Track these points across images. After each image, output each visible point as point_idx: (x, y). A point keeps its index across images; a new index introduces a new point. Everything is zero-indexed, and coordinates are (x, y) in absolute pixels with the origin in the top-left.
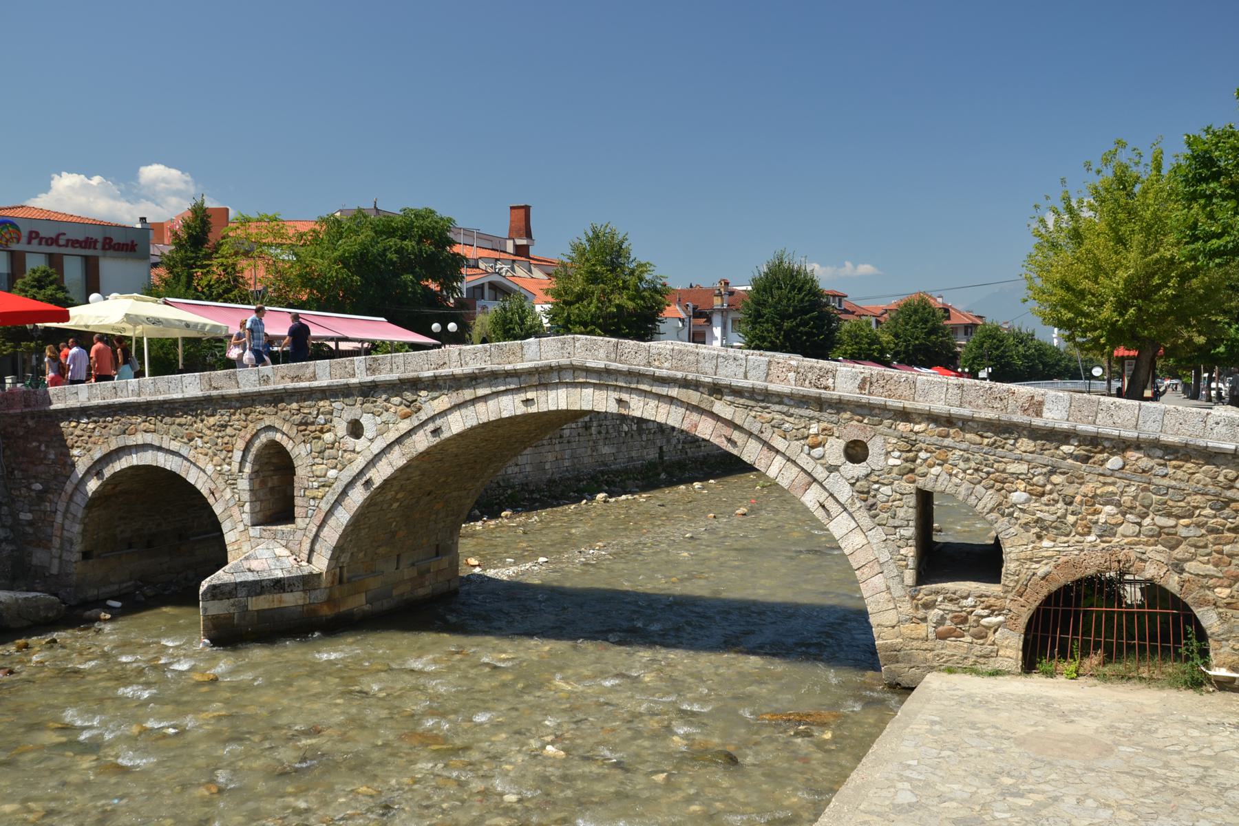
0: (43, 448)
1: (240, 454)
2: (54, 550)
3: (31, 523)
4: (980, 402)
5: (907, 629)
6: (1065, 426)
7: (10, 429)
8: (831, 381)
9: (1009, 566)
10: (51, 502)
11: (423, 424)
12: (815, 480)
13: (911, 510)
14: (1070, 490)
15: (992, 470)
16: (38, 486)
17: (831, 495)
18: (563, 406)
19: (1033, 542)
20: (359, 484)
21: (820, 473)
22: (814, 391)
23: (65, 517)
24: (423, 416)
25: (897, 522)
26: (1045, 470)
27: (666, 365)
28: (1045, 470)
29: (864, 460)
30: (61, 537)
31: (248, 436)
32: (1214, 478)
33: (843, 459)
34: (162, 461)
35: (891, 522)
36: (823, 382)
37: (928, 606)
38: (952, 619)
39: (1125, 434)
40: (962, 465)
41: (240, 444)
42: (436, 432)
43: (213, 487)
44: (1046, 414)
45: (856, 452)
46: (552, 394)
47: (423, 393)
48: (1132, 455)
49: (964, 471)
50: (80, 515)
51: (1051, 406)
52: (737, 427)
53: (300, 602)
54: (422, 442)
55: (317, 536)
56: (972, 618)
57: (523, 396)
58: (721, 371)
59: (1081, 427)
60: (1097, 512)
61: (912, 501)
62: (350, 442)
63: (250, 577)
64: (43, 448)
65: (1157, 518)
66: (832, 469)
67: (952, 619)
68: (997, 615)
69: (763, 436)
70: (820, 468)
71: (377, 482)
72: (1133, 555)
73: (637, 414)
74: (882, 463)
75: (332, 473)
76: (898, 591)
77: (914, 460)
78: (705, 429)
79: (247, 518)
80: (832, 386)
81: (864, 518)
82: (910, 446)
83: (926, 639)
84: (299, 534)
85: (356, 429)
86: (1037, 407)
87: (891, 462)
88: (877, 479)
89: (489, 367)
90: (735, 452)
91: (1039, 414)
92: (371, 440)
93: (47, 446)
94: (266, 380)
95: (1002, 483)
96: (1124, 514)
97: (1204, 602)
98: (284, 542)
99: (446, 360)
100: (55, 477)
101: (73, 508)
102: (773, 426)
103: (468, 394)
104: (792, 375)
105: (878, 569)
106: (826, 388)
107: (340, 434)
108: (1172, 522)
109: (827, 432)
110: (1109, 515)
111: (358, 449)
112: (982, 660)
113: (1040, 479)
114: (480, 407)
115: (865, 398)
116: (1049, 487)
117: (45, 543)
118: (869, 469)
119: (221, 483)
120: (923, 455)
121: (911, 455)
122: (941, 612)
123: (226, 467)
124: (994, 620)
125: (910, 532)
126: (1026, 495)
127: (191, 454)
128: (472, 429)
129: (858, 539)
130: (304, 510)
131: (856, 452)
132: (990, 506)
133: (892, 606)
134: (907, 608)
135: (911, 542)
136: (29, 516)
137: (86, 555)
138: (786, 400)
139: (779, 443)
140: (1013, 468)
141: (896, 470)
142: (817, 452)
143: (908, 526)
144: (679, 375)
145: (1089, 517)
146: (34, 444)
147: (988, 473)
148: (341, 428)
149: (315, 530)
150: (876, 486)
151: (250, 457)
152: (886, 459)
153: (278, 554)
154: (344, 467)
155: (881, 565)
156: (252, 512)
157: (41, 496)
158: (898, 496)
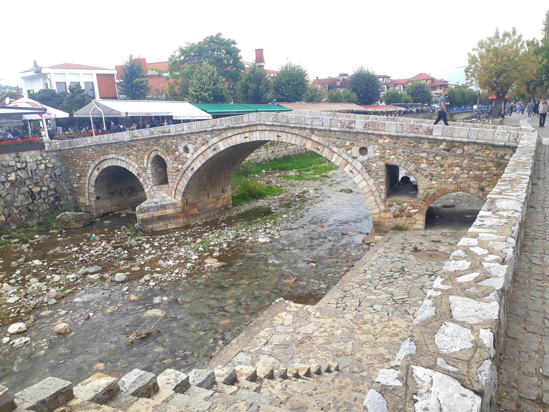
0: (78, 161)
1: (147, 160)
2: (87, 197)
3: (77, 188)
4: (409, 130)
5: (383, 215)
6: (441, 138)
7: (66, 155)
8: (354, 125)
9: (421, 191)
11: (209, 147)
12: (348, 162)
13: (383, 172)
14: (442, 163)
15: (414, 156)
16: (78, 175)
17: (354, 167)
18: (258, 139)
19: (429, 182)
22: (347, 130)
24: (209, 144)
25: (378, 177)
26: (433, 155)
27: (294, 122)
28: (433, 155)
29: (366, 154)
30: (89, 193)
31: (149, 154)
32: (496, 155)
33: (359, 154)
34: (119, 164)
35: (376, 177)
37: (390, 206)
38: (399, 211)
40: (402, 155)
41: (146, 157)
42: (214, 150)
43: (138, 173)
44: (434, 133)
46: (254, 135)
47: (209, 136)
48: (466, 148)
49: (403, 157)
50: (94, 184)
51: (436, 131)
52: (320, 144)
53: (173, 212)
54: (210, 154)
55: (176, 189)
56: (406, 210)
57: (243, 136)
58: (314, 124)
59: (447, 138)
60: (453, 170)
61: (384, 168)
62: (185, 155)
63: (154, 205)
64: (78, 161)
65: (475, 171)
66: (354, 158)
67: (399, 211)
68: (415, 209)
70: (350, 158)
71: (196, 169)
72: (466, 185)
73: (285, 141)
74: (373, 155)
75: (180, 166)
76: (379, 201)
77: (384, 153)
80: (354, 127)
81: (367, 176)
83: (390, 218)
84: (170, 189)
85: (186, 150)
87: (376, 154)
88: (371, 161)
89: (231, 126)
91: (431, 134)
93: (79, 160)
95: (417, 161)
96: (462, 170)
98: (165, 192)
99: (216, 123)
100: (83, 171)
101: (91, 182)
102: (333, 143)
103: (224, 135)
104: (339, 124)
105: (371, 194)
106: (352, 128)
107: (181, 152)
108: (480, 173)
109: (352, 144)
110: (457, 171)
111: (188, 157)
112: (410, 225)
113: (431, 159)
115: (366, 131)
116: (435, 162)
117: (83, 195)
118: (368, 158)
119: (141, 171)
120: (388, 151)
121: (383, 151)
122: (395, 208)
123: (142, 166)
124: (414, 211)
125: (383, 180)
126: (426, 165)
128: (227, 149)
129: (364, 183)
130: (171, 180)
131: (363, 151)
132: (413, 169)
133: (377, 207)
134: (382, 207)
135: (384, 184)
136: (76, 185)
137: (98, 198)
138: (337, 133)
141: (378, 157)
143: (383, 177)
144: (299, 126)
145: (450, 172)
147: (412, 157)
148: (181, 149)
149: (176, 187)
150: (371, 164)
151: (150, 161)
152: (374, 154)
153: (163, 196)
154: (184, 164)
155: (373, 192)
156: (153, 181)
158: (379, 167)
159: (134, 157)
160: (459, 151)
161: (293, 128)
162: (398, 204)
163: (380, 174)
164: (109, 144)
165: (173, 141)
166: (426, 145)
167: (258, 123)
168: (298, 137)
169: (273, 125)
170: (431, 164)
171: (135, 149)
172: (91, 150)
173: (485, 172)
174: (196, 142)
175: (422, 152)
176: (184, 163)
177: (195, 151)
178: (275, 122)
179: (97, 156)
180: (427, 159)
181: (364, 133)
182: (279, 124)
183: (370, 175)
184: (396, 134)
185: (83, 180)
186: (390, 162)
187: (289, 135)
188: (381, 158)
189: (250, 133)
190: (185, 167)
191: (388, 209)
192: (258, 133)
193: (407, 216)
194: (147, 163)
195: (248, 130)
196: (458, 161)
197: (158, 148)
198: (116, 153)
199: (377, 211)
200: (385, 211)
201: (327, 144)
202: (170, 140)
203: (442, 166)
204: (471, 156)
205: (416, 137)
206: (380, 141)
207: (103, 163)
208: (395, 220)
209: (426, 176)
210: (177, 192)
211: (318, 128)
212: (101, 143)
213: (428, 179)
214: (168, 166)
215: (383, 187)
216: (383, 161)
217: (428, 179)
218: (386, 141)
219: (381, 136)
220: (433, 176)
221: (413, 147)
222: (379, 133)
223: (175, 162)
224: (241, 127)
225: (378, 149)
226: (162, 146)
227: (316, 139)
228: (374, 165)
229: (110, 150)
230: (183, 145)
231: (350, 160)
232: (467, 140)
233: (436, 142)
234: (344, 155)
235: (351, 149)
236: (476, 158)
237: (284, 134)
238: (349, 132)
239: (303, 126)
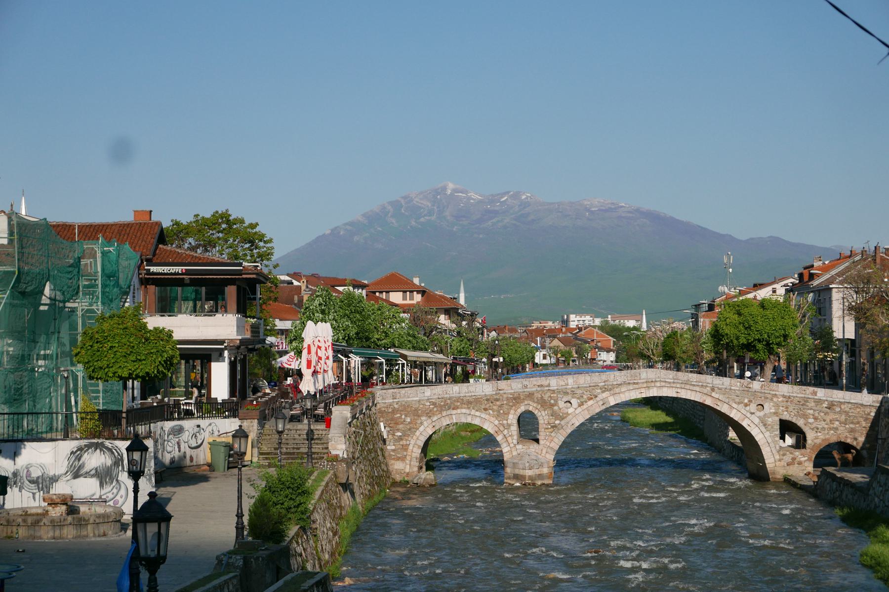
0: (403, 417)
2: (407, 462)
3: (393, 450)
4: (798, 391)
5: (778, 463)
6: (824, 399)
10: (406, 440)
16: (399, 434)
18: (655, 395)
20: (569, 425)
23: (413, 447)
27: (695, 380)
32: (864, 412)
36: (749, 386)
37: (784, 455)
39: (841, 400)
44: (818, 395)
46: (651, 391)
48: (843, 407)
59: (829, 399)
60: (833, 424)
61: (778, 423)
64: (403, 417)
66: (752, 413)
69: (729, 403)
70: (748, 413)
73: (684, 397)
74: (768, 411)
75: (557, 422)
78: (708, 402)
79: (515, 442)
82: (777, 405)
86: (815, 393)
87: (771, 411)
90: (719, 409)
91: (816, 395)
92: (576, 409)
94: (526, 387)
95: (805, 416)
100: (410, 429)
103: (617, 390)
104: (738, 384)
109: (750, 401)
111: (569, 412)
113: (817, 415)
115: (763, 391)
119: (502, 428)
120: (781, 408)
123: (505, 422)
129: (761, 436)
134: (777, 457)
136: (393, 447)
142: (748, 408)
144: (700, 384)
146: (398, 415)
157: (400, 438)
159: (493, 412)
160: (838, 409)
162: (791, 453)
163: (775, 427)
165: (552, 395)
166: (813, 404)
167: (659, 379)
168: (698, 393)
169: (674, 383)
170: (816, 419)
171: (498, 403)
172: (429, 404)
173: (857, 425)
174: (582, 397)
175: (809, 409)
176: (562, 419)
177: (580, 406)
178: (676, 379)
179: (436, 411)
180: (813, 415)
181: (761, 393)
182: (681, 382)
183: (766, 428)
184: (788, 394)
186: (784, 418)
187: (689, 391)
188: (776, 413)
189: (646, 389)
191: (781, 457)
192: (655, 389)
193: (798, 464)
194: (513, 419)
195: (645, 385)
196: (837, 416)
197: (531, 403)
198: (469, 408)
199: (772, 460)
200: (780, 460)
201: (727, 401)
202: (548, 394)
203: (824, 421)
204: (847, 413)
205: (805, 397)
206: (775, 399)
208: (788, 467)
209: (813, 429)
211: (720, 386)
212: (446, 396)
213: (814, 432)
214: (541, 422)
216: (777, 416)
217: (814, 432)
218: (779, 400)
220: (818, 429)
221: (802, 405)
222: (774, 393)
223: (551, 417)
224: (637, 383)
225: (773, 406)
226: (536, 401)
227: (717, 396)
228: (770, 420)
229: (459, 404)
230: (565, 399)
231: (749, 415)
232: (844, 400)
233: (819, 402)
234: (743, 411)
235: (749, 405)
236: (850, 414)
237: (683, 390)
239: (704, 384)
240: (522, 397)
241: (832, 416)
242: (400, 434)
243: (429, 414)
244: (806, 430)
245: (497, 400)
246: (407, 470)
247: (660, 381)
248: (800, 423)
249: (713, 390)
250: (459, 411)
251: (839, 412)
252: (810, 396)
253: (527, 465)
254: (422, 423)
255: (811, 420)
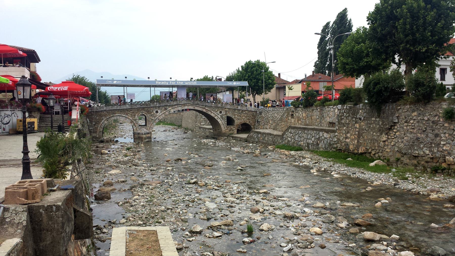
20: (157, 119)
21: (217, 115)
23: (100, 128)
41: (137, 115)
45: (221, 112)
46: (185, 107)
47: (168, 107)
48: (246, 112)
62: (156, 114)
64: (95, 117)
66: (218, 114)
75: (153, 118)
76: (225, 127)
78: (204, 111)
82: (226, 111)
84: (147, 127)
85: (157, 112)
86: (238, 107)
95: (235, 115)
97: (252, 125)
103: (174, 107)
114: (176, 109)
125: (226, 120)
127: (127, 117)
131: (221, 112)
134: (226, 129)
139: (213, 112)
140: (236, 113)
142: (217, 112)
148: (155, 112)
157: (94, 125)
160: (244, 112)
161: (200, 105)
164: (117, 109)
166: (237, 111)
171: (131, 112)
177: (161, 112)
185: (97, 125)
188: (226, 114)
190: (155, 118)
192: (187, 106)
195: (183, 105)
200: (227, 130)
207: (111, 118)
210: (150, 128)
215: (226, 123)
219: (225, 108)
224: (181, 104)
227: (207, 108)
230: (156, 110)
233: (239, 110)
238: (217, 107)
240: (140, 109)
241: (243, 115)
242: (94, 123)
243: (105, 116)
244: (235, 119)
245: (131, 111)
246: (97, 136)
247: (188, 104)
248: (233, 117)
249: (206, 106)
250: (117, 115)
251: (245, 113)
252: (236, 108)
253: (144, 133)
254: (103, 119)
255: (236, 116)
